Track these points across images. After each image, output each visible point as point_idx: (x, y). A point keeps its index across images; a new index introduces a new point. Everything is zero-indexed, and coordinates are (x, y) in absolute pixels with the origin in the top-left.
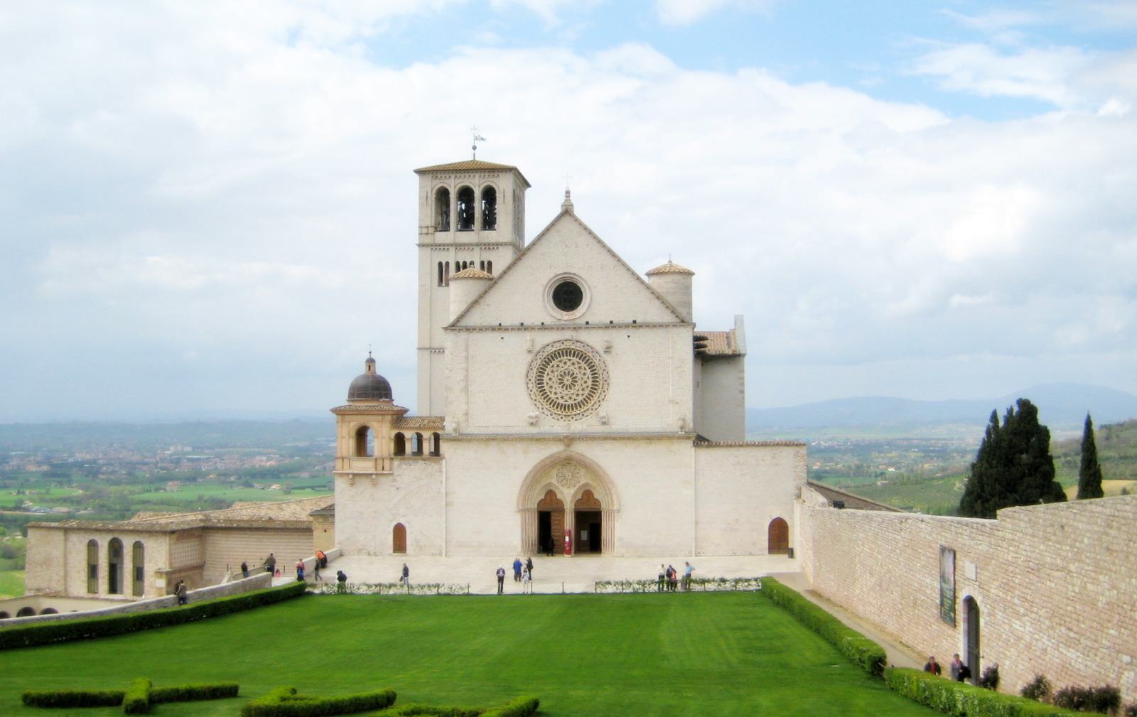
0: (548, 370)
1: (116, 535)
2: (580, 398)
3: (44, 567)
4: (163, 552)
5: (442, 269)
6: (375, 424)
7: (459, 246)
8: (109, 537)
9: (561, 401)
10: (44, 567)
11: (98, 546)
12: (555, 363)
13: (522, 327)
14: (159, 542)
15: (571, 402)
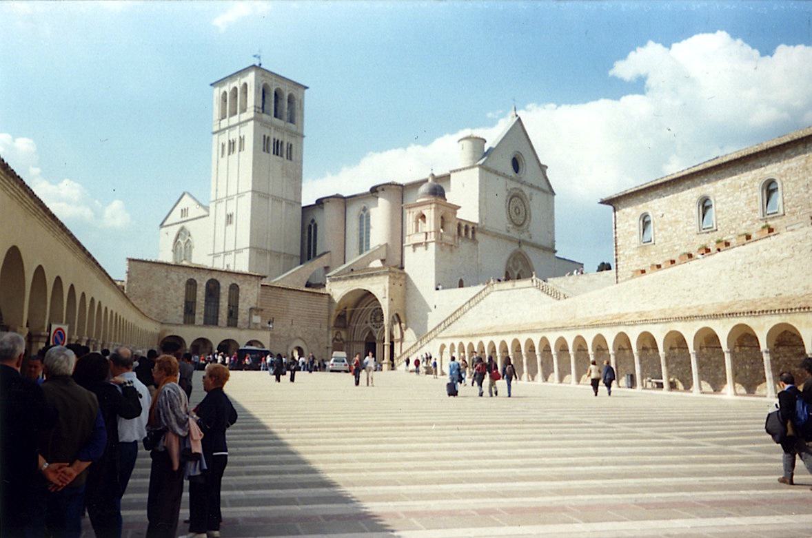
0: (511, 203)
1: (214, 277)
2: (521, 222)
3: (144, 300)
4: (255, 295)
5: (266, 140)
6: (451, 214)
7: (277, 128)
8: (208, 278)
9: (515, 221)
10: (144, 300)
11: (196, 285)
12: (513, 200)
13: (504, 176)
14: (252, 285)
15: (518, 223)
